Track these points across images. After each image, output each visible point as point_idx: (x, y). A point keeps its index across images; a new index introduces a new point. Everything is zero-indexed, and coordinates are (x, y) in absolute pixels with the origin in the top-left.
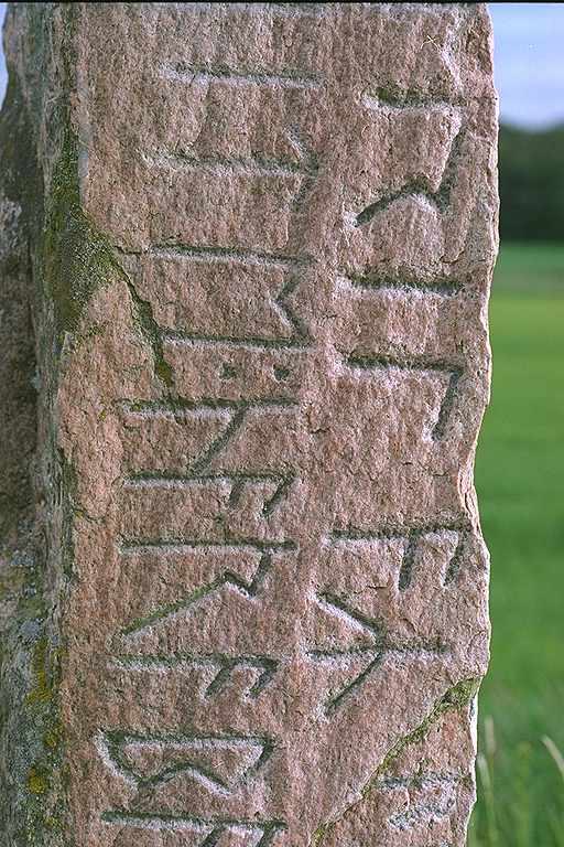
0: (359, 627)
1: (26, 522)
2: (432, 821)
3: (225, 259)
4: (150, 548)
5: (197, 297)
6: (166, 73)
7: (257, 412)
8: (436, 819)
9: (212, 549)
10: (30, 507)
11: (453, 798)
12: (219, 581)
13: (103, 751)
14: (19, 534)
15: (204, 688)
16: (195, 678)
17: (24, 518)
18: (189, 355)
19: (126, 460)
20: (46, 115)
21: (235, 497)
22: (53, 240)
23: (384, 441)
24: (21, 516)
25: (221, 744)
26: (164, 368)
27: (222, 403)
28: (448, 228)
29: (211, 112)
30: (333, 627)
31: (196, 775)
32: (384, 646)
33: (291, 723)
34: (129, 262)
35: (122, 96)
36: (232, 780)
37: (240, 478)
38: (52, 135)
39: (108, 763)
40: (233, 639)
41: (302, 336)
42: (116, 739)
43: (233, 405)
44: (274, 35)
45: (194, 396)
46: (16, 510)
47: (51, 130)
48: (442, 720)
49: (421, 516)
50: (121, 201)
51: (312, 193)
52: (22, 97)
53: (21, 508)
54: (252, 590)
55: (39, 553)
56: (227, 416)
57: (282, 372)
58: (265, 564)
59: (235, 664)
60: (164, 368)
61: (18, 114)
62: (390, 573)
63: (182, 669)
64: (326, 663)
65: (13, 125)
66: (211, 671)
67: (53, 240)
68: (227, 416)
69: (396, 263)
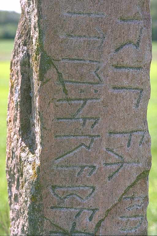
0: (117, 157)
1: (29, 132)
2: (137, 208)
3: (81, 62)
4: (62, 137)
6: (65, 13)
8: (138, 207)
9: (79, 137)
10: (30, 128)
11: (143, 202)
12: (80, 146)
14: (27, 135)
15: (77, 174)
17: (28, 131)
20: (33, 24)
21: (84, 124)
22: (36, 57)
24: (28, 130)
25: (81, 188)
26: (65, 91)
27: (80, 99)
30: (109, 157)
31: (75, 196)
34: (56, 63)
36: (84, 198)
37: (85, 119)
38: (35, 29)
39: (52, 194)
40: (84, 161)
42: (54, 187)
43: (83, 100)
44: (93, 3)
46: (26, 129)
47: (35, 28)
48: (139, 181)
50: (52, 47)
51: (103, 44)
52: (26, 18)
53: (28, 128)
54: (89, 148)
55: (33, 140)
56: (82, 102)
57: (96, 91)
59: (85, 167)
60: (65, 91)
61: (25, 22)
62: (124, 143)
63: (71, 169)
64: (109, 166)
65: (23, 25)
66: (78, 170)
67: (36, 57)
68: (82, 102)
69: (125, 62)
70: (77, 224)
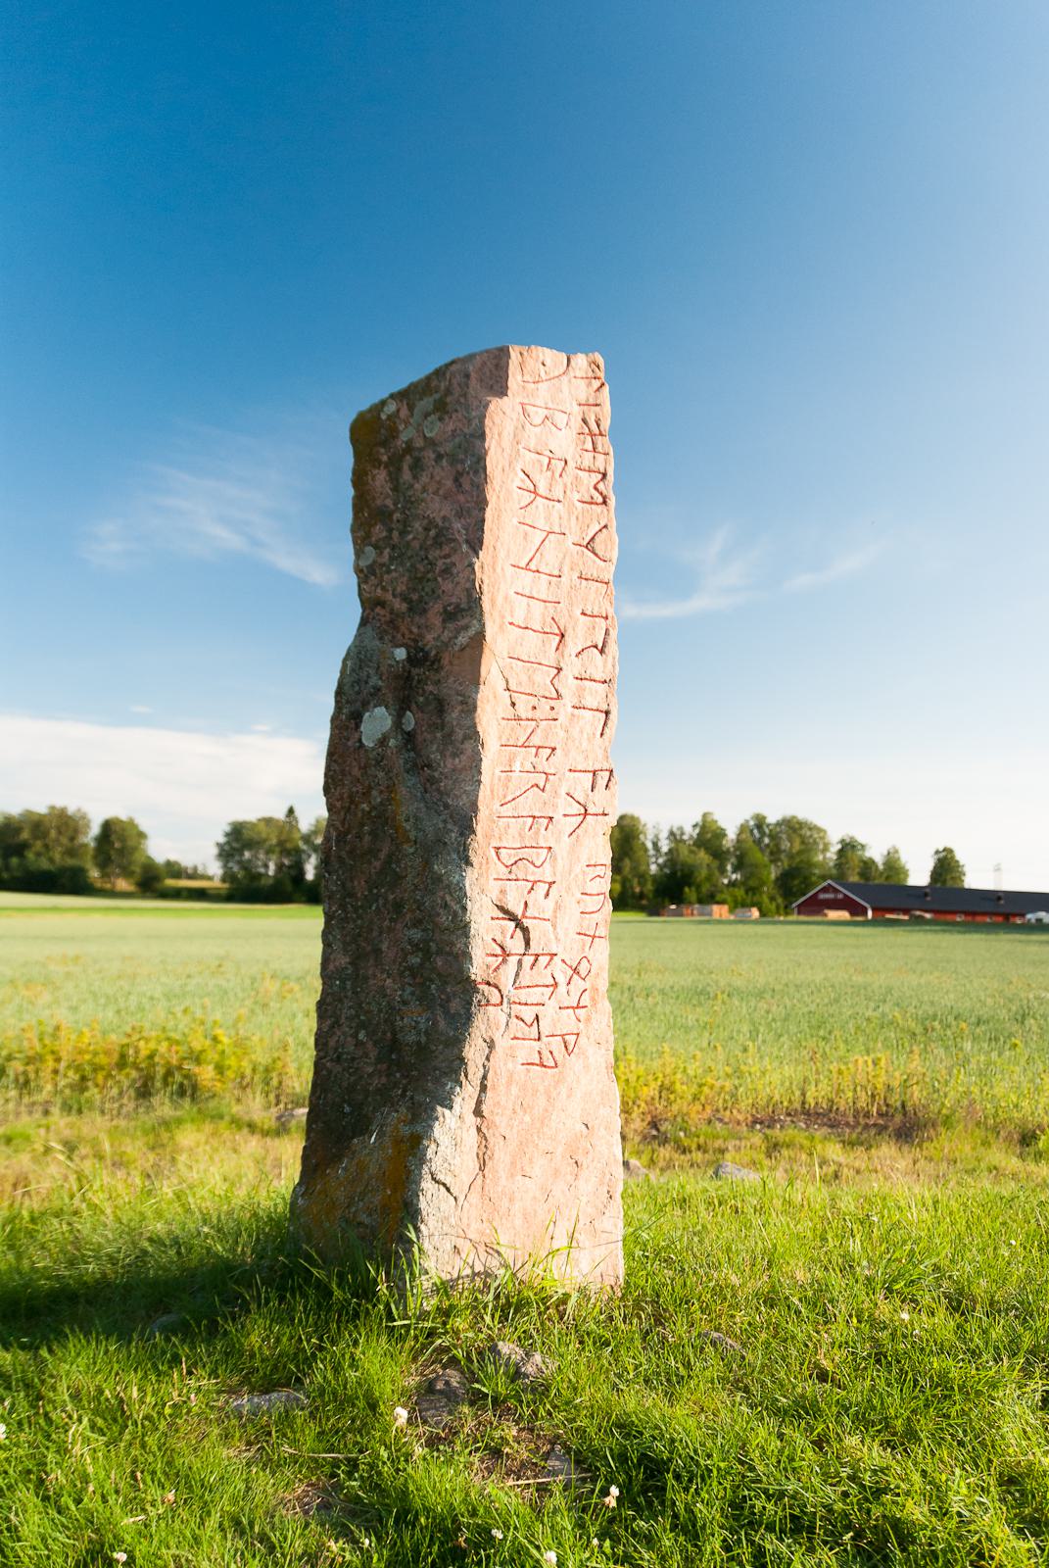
5: (524, 678)
7: (545, 722)
13: (493, 852)
16: (525, 823)
18: (520, 699)
19: (500, 738)
23: (585, 736)
28: (605, 662)
29: (529, 612)
32: (586, 814)
33: (558, 841)
35: (500, 600)
41: (559, 696)
45: (524, 717)
49: (597, 767)
54: (543, 790)
57: (552, 708)
58: (547, 780)
70: (530, 904)
